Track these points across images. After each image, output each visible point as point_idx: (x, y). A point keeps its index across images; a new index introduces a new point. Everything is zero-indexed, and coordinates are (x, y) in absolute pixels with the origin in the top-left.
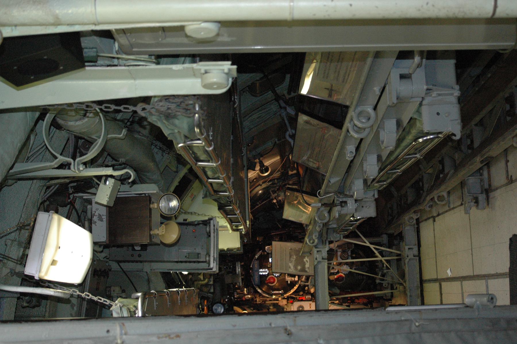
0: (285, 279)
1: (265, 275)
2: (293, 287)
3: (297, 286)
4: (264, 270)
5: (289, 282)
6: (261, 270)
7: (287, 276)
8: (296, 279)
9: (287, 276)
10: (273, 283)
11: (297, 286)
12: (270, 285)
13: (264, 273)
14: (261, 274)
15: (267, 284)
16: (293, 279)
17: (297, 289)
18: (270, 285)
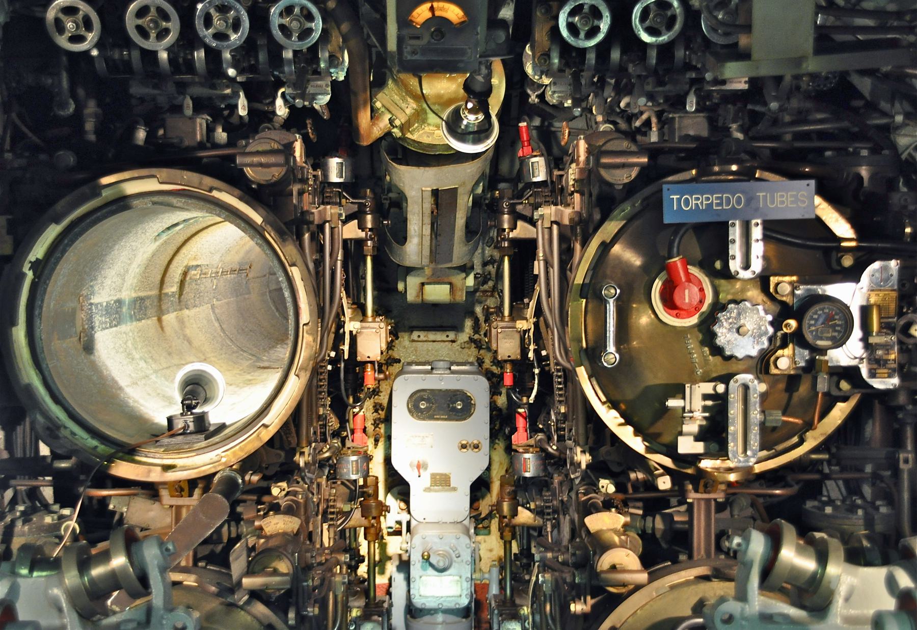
0: (694, 382)
1: (725, 257)
2: (628, 420)
3: (637, 444)
4: (758, 249)
5: (672, 403)
6: (757, 232)
7: (708, 388)
8: (687, 446)
9: (708, 388)
10: (669, 302)
11: (637, 444)
12: (658, 285)
13: (735, 250)
14: (735, 233)
15: (656, 263)
16: (692, 427)
17: (615, 438)
18: (658, 285)
